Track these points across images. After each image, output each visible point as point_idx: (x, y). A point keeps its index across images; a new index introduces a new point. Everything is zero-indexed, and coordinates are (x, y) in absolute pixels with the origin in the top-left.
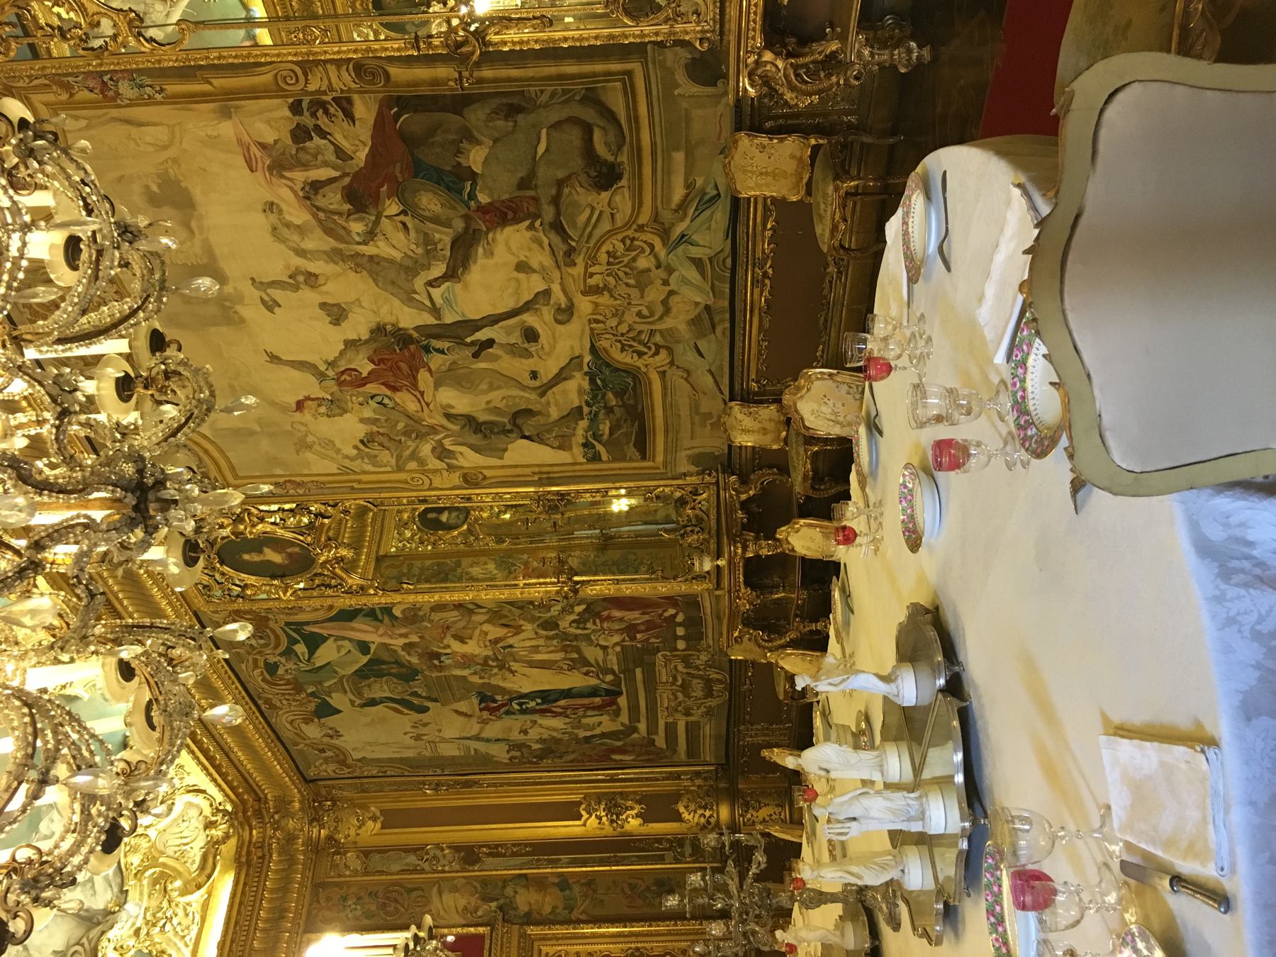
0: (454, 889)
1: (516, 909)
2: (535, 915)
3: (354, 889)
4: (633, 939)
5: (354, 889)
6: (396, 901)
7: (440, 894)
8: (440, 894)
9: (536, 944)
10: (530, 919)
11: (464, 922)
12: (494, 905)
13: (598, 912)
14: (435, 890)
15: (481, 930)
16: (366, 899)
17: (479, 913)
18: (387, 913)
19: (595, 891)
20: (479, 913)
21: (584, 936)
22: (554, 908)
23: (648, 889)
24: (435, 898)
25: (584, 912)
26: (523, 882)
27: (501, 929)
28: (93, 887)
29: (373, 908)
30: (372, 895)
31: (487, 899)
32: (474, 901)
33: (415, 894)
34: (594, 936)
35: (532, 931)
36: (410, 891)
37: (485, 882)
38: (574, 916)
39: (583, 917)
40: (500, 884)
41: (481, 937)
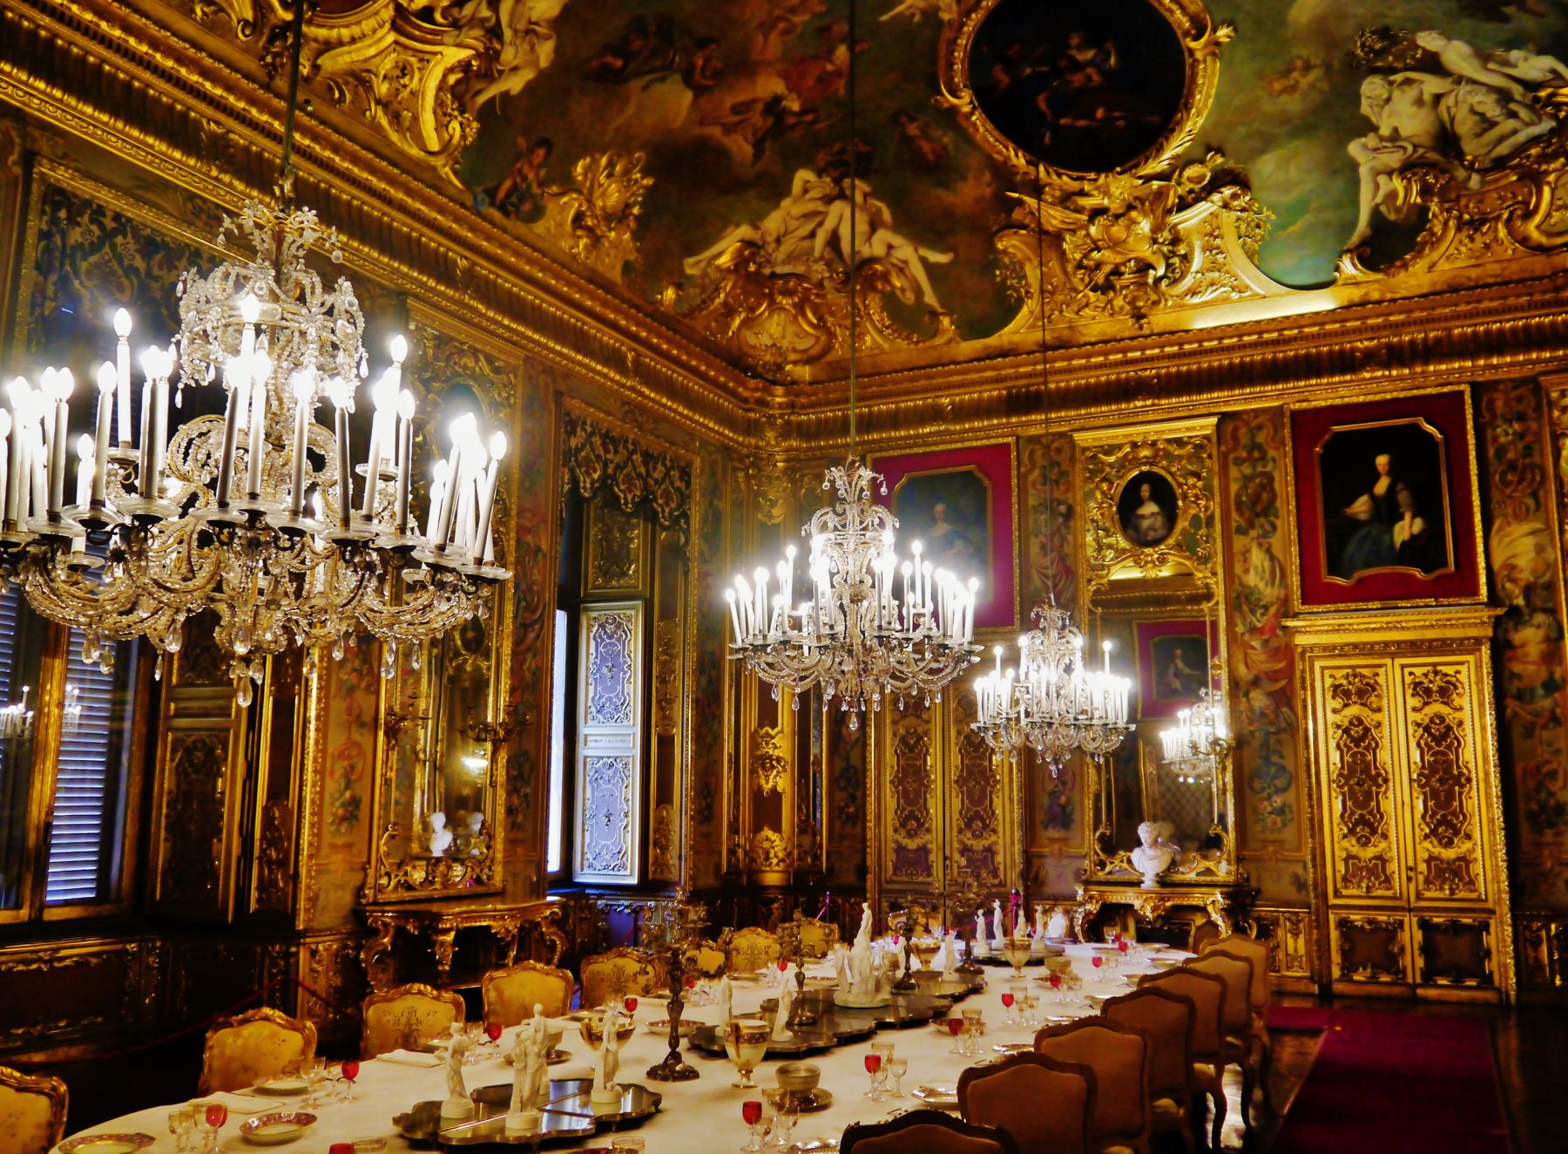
0: (1540, 549)
1: (1516, 629)
2: (1509, 654)
3: (1534, 426)
4: (1481, 775)
5: (1534, 426)
6: (1520, 481)
7: (1533, 533)
8: (1533, 533)
9: (1470, 658)
10: (1502, 650)
11: (1497, 565)
12: (1520, 601)
13: (1517, 731)
14: (1538, 525)
15: (1484, 590)
16: (1520, 445)
17: (1508, 586)
18: (1503, 474)
19: (1545, 727)
20: (1508, 586)
21: (1482, 715)
22: (1519, 677)
23: (1552, 794)
24: (1526, 527)
25: (1515, 714)
26: (1554, 634)
27: (1486, 614)
28: (1484, 131)
29: (1511, 455)
30: (1528, 451)
31: (1528, 591)
32: (1526, 576)
33: (1531, 502)
34: (1483, 728)
35: (1485, 652)
36: (1535, 495)
37: (1551, 587)
38: (1512, 705)
39: (1509, 712)
40: (1550, 605)
41: (1474, 591)
